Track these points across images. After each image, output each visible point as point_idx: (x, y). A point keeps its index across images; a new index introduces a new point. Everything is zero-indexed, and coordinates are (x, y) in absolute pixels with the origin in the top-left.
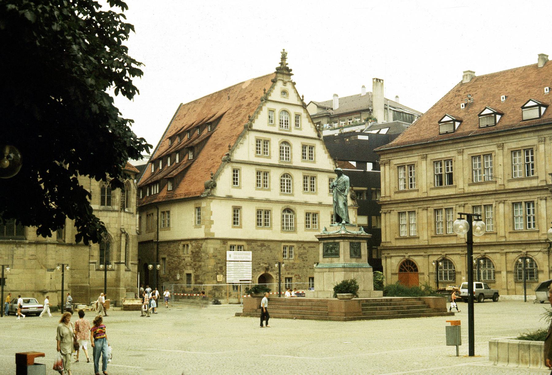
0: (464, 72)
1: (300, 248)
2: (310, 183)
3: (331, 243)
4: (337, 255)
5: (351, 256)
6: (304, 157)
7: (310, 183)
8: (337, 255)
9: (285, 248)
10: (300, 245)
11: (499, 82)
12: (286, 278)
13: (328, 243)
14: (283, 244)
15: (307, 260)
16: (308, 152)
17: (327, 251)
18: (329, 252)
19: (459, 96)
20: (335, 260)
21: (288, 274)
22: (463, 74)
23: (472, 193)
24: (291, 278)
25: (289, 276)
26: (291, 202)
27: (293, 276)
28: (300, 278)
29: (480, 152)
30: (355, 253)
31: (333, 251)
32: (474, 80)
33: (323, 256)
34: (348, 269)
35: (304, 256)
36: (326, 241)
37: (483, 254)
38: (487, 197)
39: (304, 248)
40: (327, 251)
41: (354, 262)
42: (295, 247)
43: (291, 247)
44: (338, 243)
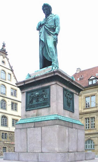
0: (77, 69)
1: (9, 134)
2: (14, 106)
3: (37, 90)
4: (46, 104)
5: (65, 108)
6: (12, 94)
7: (14, 106)
8: (46, 104)
9: (3, 133)
10: (10, 133)
11: (93, 71)
12: (3, 147)
13: (32, 91)
14: (2, 132)
15: (13, 140)
16: (14, 93)
17: (31, 102)
18: (34, 102)
19: (76, 77)
20: (43, 111)
21: (4, 145)
22: (77, 70)
23: (86, 112)
24: (6, 147)
25: (5, 146)
26: (6, 113)
27: (7, 146)
28: (10, 147)
29: (90, 94)
30: (69, 104)
31: (41, 100)
32: (81, 72)
33: (26, 109)
34: (63, 123)
35: (11, 138)
36: (29, 89)
37: (89, 138)
38: (92, 114)
39: (12, 135)
40: (31, 102)
41: (66, 116)
42: (7, 134)
43: (6, 134)
44: (49, 87)
